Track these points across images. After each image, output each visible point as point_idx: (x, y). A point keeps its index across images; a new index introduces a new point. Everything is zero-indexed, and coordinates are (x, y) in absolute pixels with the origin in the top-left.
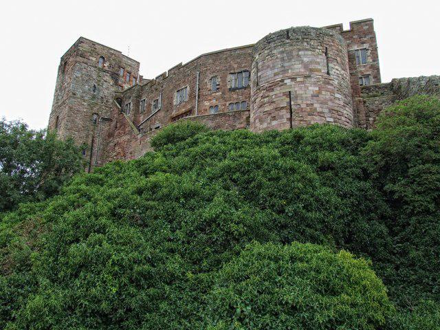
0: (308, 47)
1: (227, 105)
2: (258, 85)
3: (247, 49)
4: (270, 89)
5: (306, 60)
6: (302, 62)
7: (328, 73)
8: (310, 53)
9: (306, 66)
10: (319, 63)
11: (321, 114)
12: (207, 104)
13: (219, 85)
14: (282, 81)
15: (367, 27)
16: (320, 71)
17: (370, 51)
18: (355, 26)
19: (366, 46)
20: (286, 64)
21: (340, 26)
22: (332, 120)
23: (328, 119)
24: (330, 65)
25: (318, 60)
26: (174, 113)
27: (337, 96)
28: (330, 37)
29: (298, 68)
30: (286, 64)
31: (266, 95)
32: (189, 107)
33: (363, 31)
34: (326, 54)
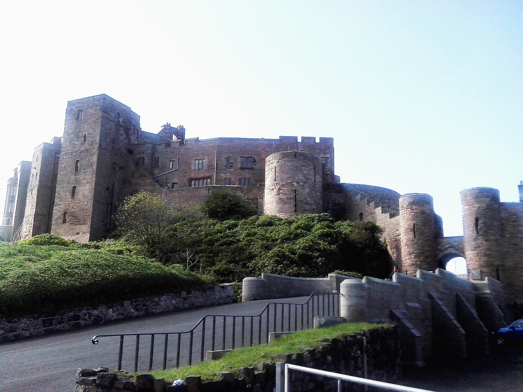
7: (315, 181)
10: (310, 175)
11: (310, 204)
16: (311, 179)
22: (315, 207)
26: (193, 176)
32: (208, 174)
34: (315, 169)
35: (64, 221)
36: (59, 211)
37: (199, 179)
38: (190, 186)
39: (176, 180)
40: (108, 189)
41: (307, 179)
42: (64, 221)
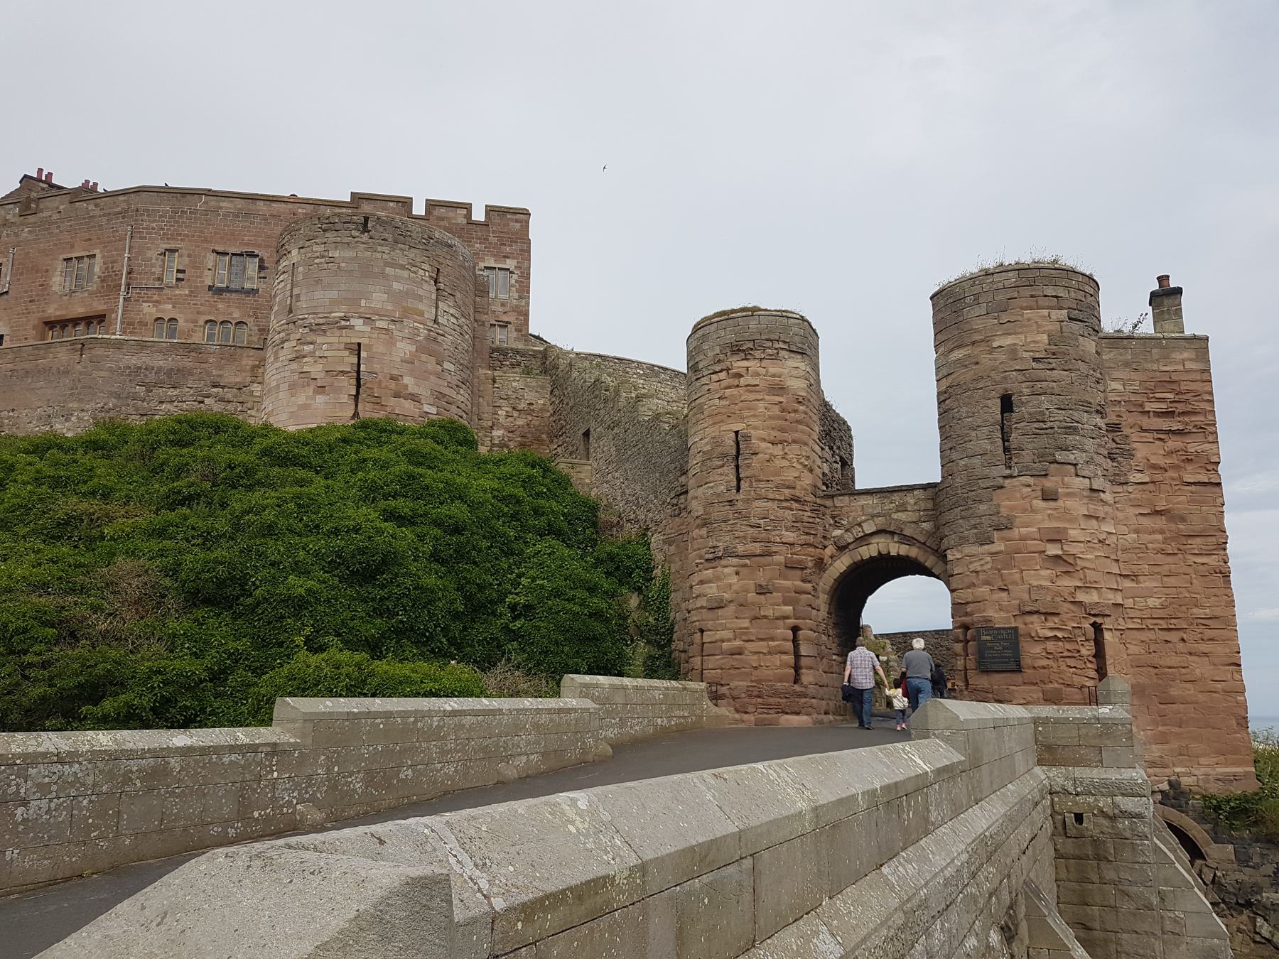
0: (403, 261)
1: (201, 323)
2: (290, 311)
3: (262, 203)
7: (435, 321)
8: (406, 274)
9: (394, 296)
10: (420, 298)
11: (415, 398)
12: (148, 310)
13: (183, 272)
14: (346, 319)
15: (518, 225)
16: (422, 314)
17: (515, 277)
18: (496, 218)
19: (510, 264)
21: (468, 207)
23: (426, 408)
24: (441, 304)
25: (420, 292)
27: (447, 365)
28: (446, 249)
29: (378, 299)
31: (309, 340)
32: (99, 306)
33: (509, 228)
34: (436, 282)
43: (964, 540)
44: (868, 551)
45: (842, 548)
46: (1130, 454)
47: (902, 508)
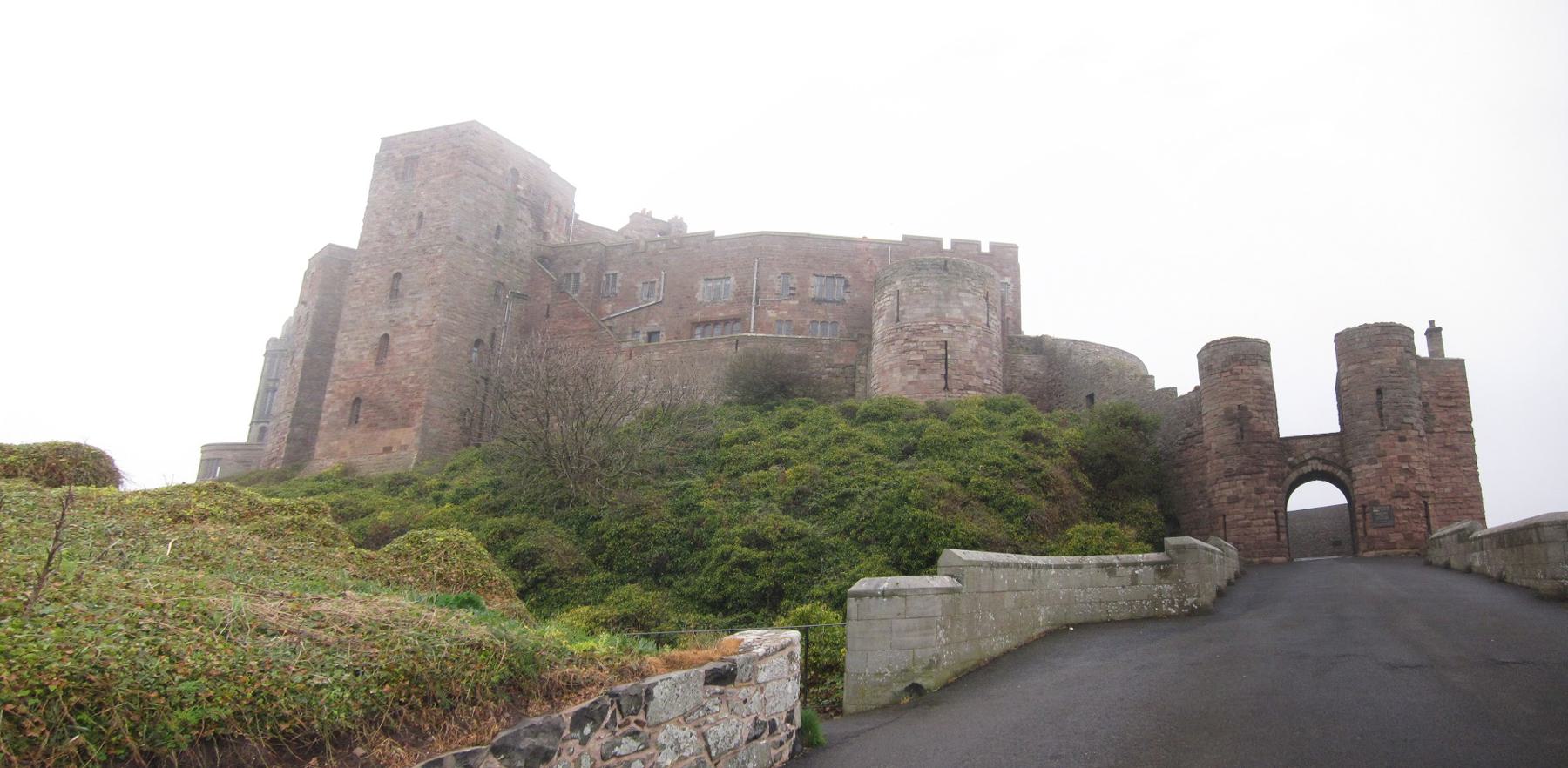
4: (918, 333)
5: (966, 304)
6: (962, 307)
9: (966, 312)
11: (979, 375)
20: (942, 304)
26: (698, 316)
29: (957, 313)
30: (942, 304)
32: (734, 312)
35: (354, 420)
36: (340, 396)
37: (716, 323)
38: (692, 336)
39: (654, 325)
40: (478, 342)
41: (971, 319)
42: (354, 420)
43: (1361, 462)
44: (1306, 469)
45: (1293, 467)
46: (1433, 418)
47: (1324, 446)
